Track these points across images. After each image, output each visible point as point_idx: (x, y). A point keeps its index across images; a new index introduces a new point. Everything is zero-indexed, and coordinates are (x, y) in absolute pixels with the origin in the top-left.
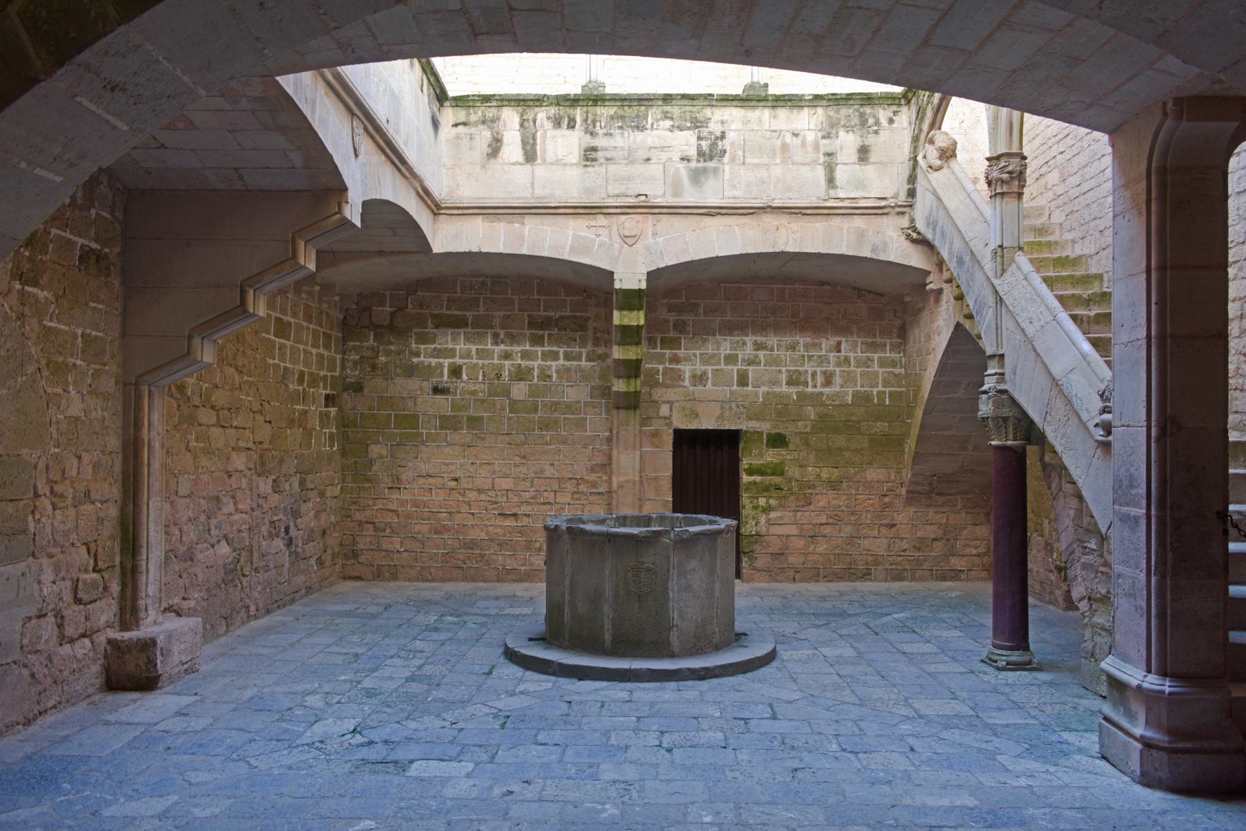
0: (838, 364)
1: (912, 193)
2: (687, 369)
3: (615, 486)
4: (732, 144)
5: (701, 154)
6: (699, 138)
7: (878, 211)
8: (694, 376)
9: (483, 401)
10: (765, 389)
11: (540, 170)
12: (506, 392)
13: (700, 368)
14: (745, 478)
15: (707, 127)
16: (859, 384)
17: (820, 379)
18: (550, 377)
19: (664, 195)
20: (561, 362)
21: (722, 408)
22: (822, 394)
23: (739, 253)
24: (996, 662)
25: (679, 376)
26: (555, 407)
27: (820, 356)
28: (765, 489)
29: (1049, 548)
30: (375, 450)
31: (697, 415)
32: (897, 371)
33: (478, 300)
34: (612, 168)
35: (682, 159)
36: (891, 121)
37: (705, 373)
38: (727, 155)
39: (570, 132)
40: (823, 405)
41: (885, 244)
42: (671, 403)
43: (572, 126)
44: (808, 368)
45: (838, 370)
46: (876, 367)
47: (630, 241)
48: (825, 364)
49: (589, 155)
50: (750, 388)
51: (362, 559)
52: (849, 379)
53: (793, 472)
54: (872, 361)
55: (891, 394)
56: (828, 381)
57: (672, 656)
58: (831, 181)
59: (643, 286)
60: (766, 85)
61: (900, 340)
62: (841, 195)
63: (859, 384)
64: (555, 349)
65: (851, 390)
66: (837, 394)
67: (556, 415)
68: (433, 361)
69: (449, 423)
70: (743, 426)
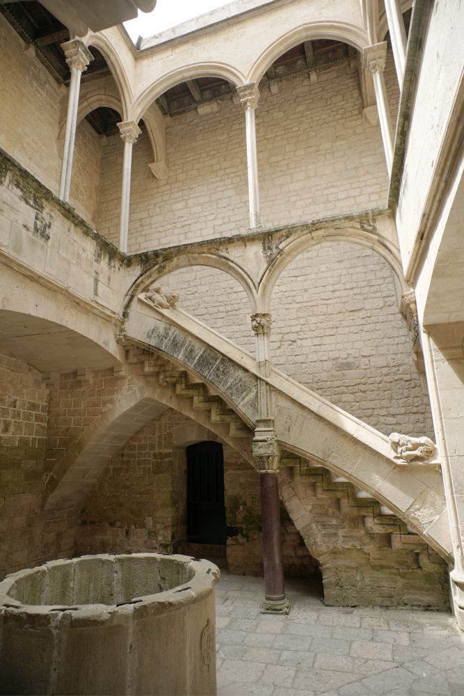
0: (14, 417)
1: (125, 315)
4: (54, 234)
5: (36, 229)
6: (36, 218)
15: (41, 212)
16: (23, 432)
23: (42, 317)
24: (281, 610)
27: (4, 409)
29: (153, 534)
32: (43, 424)
35: (25, 226)
36: (119, 269)
38: (50, 240)
45: (13, 420)
48: (6, 416)
52: (18, 427)
54: (32, 416)
55: (39, 439)
60: (74, 209)
61: (46, 404)
63: (23, 432)
65: (18, 436)
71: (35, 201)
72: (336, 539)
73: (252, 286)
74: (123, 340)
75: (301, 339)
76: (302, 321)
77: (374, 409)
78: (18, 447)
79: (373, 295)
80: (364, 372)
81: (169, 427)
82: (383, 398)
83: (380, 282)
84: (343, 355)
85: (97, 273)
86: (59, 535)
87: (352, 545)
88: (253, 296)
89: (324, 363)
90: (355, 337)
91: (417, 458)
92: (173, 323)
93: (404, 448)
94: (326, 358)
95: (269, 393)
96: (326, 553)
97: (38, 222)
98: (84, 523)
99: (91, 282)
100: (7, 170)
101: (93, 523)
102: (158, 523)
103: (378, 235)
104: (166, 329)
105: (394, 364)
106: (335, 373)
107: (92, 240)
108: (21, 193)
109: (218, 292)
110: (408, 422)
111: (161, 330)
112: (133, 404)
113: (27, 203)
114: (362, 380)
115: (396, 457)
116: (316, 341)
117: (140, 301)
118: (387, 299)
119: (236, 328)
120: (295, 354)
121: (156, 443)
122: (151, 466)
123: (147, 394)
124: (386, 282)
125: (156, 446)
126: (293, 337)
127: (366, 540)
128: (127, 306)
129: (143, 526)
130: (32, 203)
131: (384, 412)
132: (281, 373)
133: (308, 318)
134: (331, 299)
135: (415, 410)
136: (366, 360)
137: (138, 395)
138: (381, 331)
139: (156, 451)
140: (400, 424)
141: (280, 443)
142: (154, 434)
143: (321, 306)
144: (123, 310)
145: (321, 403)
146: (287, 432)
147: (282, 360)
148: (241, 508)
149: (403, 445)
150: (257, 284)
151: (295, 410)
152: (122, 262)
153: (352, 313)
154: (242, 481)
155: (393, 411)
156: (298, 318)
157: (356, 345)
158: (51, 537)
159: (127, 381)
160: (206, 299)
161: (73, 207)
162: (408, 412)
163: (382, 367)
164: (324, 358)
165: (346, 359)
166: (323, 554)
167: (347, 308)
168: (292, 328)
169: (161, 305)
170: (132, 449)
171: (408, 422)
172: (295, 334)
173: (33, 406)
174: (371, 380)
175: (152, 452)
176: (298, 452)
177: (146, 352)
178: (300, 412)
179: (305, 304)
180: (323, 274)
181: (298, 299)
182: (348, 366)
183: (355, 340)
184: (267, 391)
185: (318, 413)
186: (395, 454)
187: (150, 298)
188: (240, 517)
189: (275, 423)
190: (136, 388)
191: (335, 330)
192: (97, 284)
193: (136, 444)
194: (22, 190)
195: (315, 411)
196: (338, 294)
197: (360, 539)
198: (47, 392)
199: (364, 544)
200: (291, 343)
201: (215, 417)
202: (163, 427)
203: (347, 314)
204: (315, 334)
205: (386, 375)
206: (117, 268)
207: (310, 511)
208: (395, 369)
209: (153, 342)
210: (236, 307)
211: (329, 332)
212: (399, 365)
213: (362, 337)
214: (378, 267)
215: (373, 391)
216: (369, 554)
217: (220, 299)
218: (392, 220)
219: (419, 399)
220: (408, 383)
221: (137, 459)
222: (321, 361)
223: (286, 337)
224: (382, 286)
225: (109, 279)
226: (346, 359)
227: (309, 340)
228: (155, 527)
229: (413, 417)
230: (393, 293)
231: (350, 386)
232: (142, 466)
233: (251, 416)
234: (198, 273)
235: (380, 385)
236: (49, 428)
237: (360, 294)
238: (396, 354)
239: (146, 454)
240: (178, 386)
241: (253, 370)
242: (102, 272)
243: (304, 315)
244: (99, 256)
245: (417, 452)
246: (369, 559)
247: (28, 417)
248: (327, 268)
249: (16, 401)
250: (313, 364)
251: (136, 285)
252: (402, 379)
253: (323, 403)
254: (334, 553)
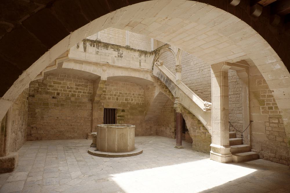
0: (134, 98)
1: (153, 69)
2: (107, 97)
3: (93, 119)
5: (118, 56)
6: (118, 53)
7: (147, 71)
8: (108, 98)
9: (64, 101)
10: (121, 101)
11: (87, 54)
12: (70, 99)
13: (109, 96)
14: (118, 118)
17: (131, 100)
18: (80, 96)
19: (111, 63)
20: (82, 93)
21: (114, 104)
22: (131, 103)
25: (105, 98)
26: (80, 102)
28: (121, 120)
30: (37, 110)
31: (109, 106)
32: (143, 99)
33: (64, 79)
34: (102, 56)
35: (115, 57)
36: (149, 56)
37: (110, 98)
39: (94, 48)
40: (131, 104)
41: (148, 77)
42: (104, 103)
43: (94, 46)
44: (129, 98)
45: (134, 98)
46: (140, 98)
47: (104, 71)
49: (97, 53)
50: (118, 101)
51: (32, 136)
52: (135, 100)
53: (126, 117)
56: (132, 101)
57: (128, 151)
58: (140, 65)
59: (106, 80)
62: (142, 68)
64: (81, 91)
66: (133, 103)
67: (81, 104)
68: (53, 91)
69: (56, 105)
70: (117, 108)
71: (117, 50)
75: (205, 69)
78: (136, 105)
85: (140, 60)
86: (151, 127)
92: (161, 71)
97: (119, 54)
98: (158, 125)
99: (139, 63)
100: (109, 46)
101: (160, 125)
104: (160, 72)
107: (137, 52)
108: (113, 50)
111: (159, 73)
112: (158, 93)
113: (115, 51)
115: (204, 109)
117: (155, 65)
119: (188, 67)
123: (160, 91)
126: (202, 68)
128: (153, 66)
129: (169, 127)
130: (116, 50)
144: (152, 68)
146: (181, 101)
147: (199, 77)
151: (183, 95)
152: (151, 54)
158: (148, 127)
161: (129, 45)
172: (203, 67)
173: (139, 95)
177: (158, 79)
187: (157, 63)
189: (180, 98)
190: (158, 89)
192: (140, 63)
193: (167, 104)
194: (113, 49)
198: (144, 91)
201: (171, 97)
206: (148, 56)
209: (158, 76)
210: (188, 60)
219: (238, 88)
223: (201, 68)
225: (145, 60)
229: (236, 96)
233: (175, 97)
236: (145, 100)
242: (142, 59)
244: (141, 55)
245: (208, 108)
247: (138, 97)
249: (134, 94)
251: (154, 60)
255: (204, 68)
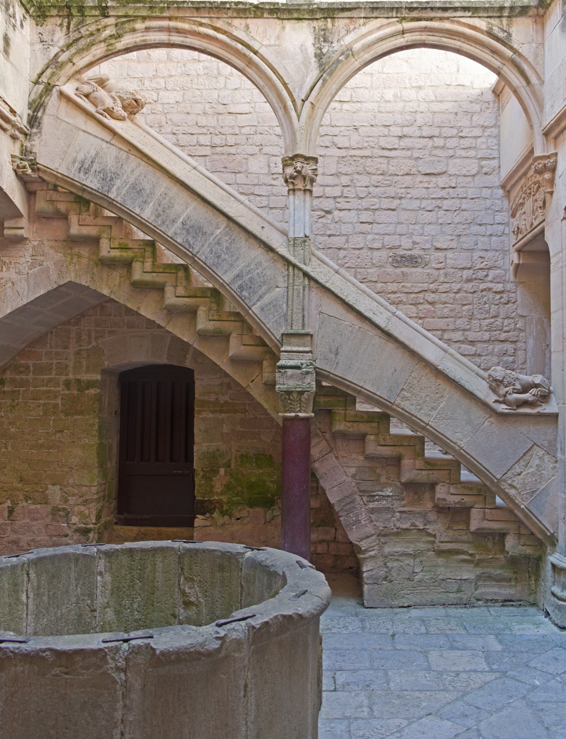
72: (389, 516)
73: (289, 103)
74: (29, 171)
75: (340, 210)
76: (345, 180)
77: (444, 330)
79: (463, 153)
80: (436, 273)
81: (96, 338)
82: (460, 315)
83: (477, 132)
84: (406, 243)
87: (412, 525)
88: (291, 123)
89: (376, 253)
90: (431, 217)
91: (526, 403)
93: (510, 389)
94: (379, 246)
95: (307, 289)
96: (373, 535)
102: (73, 495)
103: (511, 48)
105: (482, 266)
106: (390, 269)
109: (199, 108)
110: (492, 353)
114: (432, 286)
115: (496, 401)
116: (365, 216)
118: (484, 163)
120: (329, 233)
121: (71, 364)
122: (59, 401)
123: (71, 277)
124: (486, 134)
125: (71, 369)
127: (432, 516)
131: (458, 336)
132: (327, 260)
133: (356, 176)
134: (395, 149)
135: (503, 336)
136: (440, 254)
137: (54, 276)
138: (469, 213)
139: (71, 376)
140: (479, 355)
141: (320, 375)
142: (66, 348)
143: (379, 160)
145: (390, 314)
146: (333, 356)
148: (222, 471)
149: (509, 384)
150: (299, 102)
153: (426, 178)
154: (226, 429)
155: (471, 336)
156: (337, 175)
157: (428, 229)
159: (29, 246)
160: (176, 118)
162: (492, 339)
163: (464, 269)
164: (377, 245)
165: (410, 250)
166: (368, 537)
167: (420, 169)
168: (327, 189)
169: (109, 112)
170: (21, 372)
171: (492, 353)
172: (331, 201)
174: (442, 288)
175: (63, 378)
176: (348, 387)
178: (358, 323)
179: (353, 152)
180: (389, 105)
181: (340, 140)
182: (413, 261)
183: (426, 221)
184: (304, 287)
185: (386, 329)
186: (495, 398)
188: (218, 487)
191: (397, 202)
195: (382, 325)
196: (406, 143)
197: (424, 515)
199: (429, 522)
200: (323, 213)
202: (84, 337)
203: (420, 178)
204: (365, 204)
205: (469, 280)
207: (353, 476)
208: (481, 274)
210: (231, 140)
211: (386, 203)
212: (489, 269)
213: (438, 218)
214: (477, 107)
215: (446, 303)
216: (435, 536)
217: (203, 121)
218: (539, 27)
220: (498, 296)
221: (31, 389)
222: (371, 249)
224: (479, 140)
226: (410, 250)
227: (353, 213)
228: (66, 501)
230: (495, 154)
231: (411, 293)
232: (41, 402)
234: (161, 66)
235: (457, 296)
237: (443, 147)
238: (487, 250)
239: (50, 380)
240: (137, 266)
241: (283, 251)
243: (349, 170)
246: (433, 542)
248: (395, 96)
250: (357, 252)
252: (490, 289)
253: (394, 314)
254: (385, 535)
255: (338, 205)
